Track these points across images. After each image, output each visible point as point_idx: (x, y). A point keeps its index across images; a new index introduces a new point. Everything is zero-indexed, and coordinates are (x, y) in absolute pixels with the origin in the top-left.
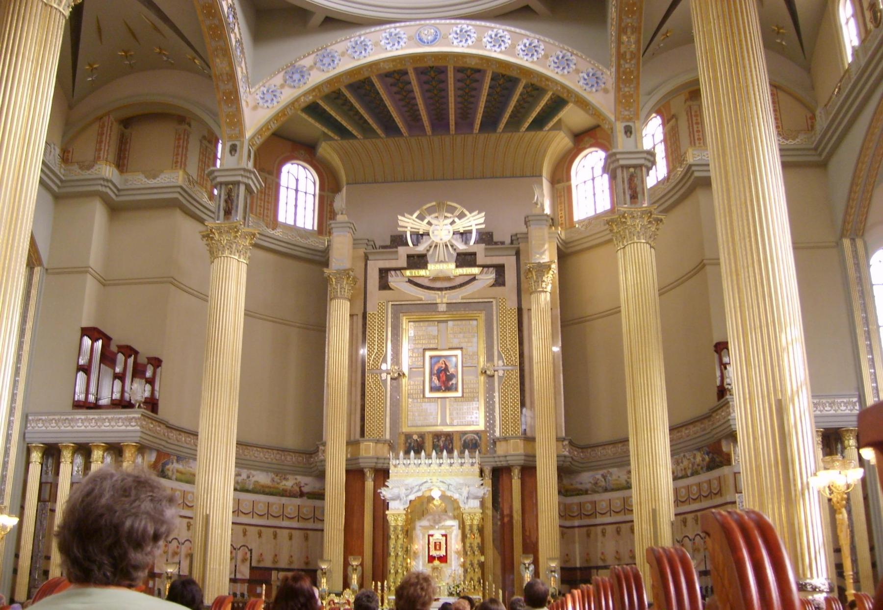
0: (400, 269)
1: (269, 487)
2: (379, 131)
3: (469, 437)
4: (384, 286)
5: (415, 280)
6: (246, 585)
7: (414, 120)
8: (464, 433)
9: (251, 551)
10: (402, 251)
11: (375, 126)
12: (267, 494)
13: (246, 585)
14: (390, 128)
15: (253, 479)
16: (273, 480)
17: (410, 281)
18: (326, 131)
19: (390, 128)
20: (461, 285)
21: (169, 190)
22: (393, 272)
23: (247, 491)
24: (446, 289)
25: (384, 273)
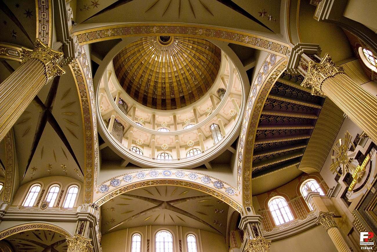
0: (347, 188)
2: (304, 146)
5: (355, 188)
11: (302, 147)
20: (370, 171)
21: (300, 227)
24: (367, 179)
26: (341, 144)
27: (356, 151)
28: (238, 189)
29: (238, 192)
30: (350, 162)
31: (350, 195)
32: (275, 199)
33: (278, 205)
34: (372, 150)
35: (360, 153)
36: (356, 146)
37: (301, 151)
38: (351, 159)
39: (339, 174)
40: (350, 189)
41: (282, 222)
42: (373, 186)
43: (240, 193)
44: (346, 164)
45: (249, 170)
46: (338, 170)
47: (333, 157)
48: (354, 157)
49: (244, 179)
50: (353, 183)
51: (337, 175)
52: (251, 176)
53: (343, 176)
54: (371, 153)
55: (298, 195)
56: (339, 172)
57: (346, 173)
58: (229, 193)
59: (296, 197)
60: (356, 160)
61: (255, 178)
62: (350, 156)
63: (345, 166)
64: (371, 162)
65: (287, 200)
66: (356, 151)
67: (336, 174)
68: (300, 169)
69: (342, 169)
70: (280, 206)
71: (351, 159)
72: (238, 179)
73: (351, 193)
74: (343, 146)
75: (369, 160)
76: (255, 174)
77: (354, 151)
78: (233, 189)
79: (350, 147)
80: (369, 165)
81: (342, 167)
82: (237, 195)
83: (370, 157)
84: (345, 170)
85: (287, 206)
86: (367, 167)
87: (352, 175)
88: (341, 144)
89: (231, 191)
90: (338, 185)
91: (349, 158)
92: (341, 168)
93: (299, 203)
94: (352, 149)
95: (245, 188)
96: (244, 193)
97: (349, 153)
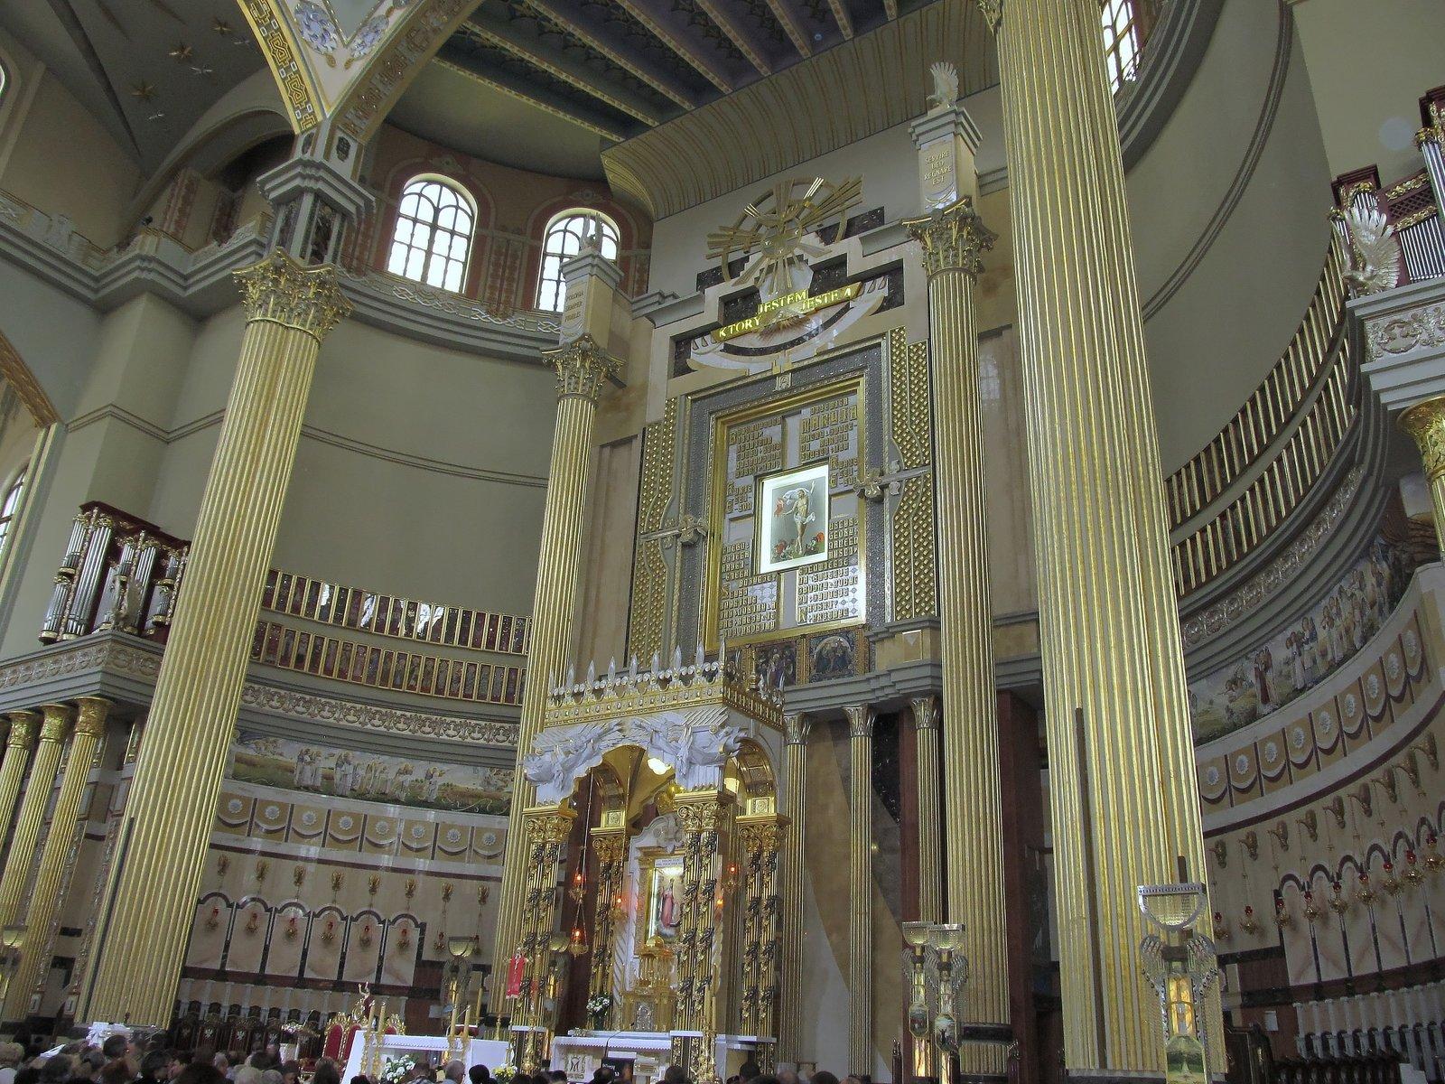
1: (477, 796)
2: (686, 106)
3: (832, 642)
4: (680, 368)
6: (404, 999)
7: (735, 66)
8: (821, 636)
9: (422, 927)
10: (714, 293)
12: (471, 810)
13: (404, 999)
14: (699, 89)
15: (440, 781)
16: (487, 782)
17: (730, 349)
18: (605, 133)
19: (699, 89)
22: (698, 341)
23: (426, 804)
25: (682, 344)
26: (810, 193)
27: (836, 249)
28: (354, 45)
29: (342, 56)
30: (791, 262)
31: (707, 349)
32: (442, 184)
33: (437, 211)
34: (879, 281)
35: (841, 262)
36: (847, 235)
37: (663, 108)
38: (800, 257)
39: (725, 272)
40: (722, 333)
41: (414, 274)
42: (793, 371)
43: (348, 64)
44: (773, 261)
45: (452, 13)
46: (733, 257)
47: (750, 210)
48: (813, 261)
49: (409, 33)
50: (748, 324)
51: (718, 269)
52: (439, 41)
53: (735, 285)
54: (868, 284)
55: (529, 231)
56: (730, 265)
57: (750, 283)
58: (306, 32)
59: (520, 232)
60: (810, 275)
61: (446, 65)
62: (804, 247)
63: (764, 265)
64: (847, 309)
65: (483, 221)
66: (836, 249)
67: (717, 262)
68: (605, 161)
69: (747, 266)
70: (445, 219)
71: (800, 257)
72: (382, 11)
73: (711, 346)
74: (811, 206)
75: (848, 299)
76: (460, 50)
77: (827, 244)
78: (330, 27)
79: (827, 223)
80: (832, 312)
81: (753, 259)
82: (331, 61)
83: (857, 295)
84: (757, 274)
85: (469, 238)
86: (821, 313)
87: (760, 302)
88: (810, 193)
89: (317, 29)
90: (699, 299)
91: (797, 252)
92: (747, 259)
93: (515, 257)
94: (827, 235)
95: (388, 64)
96: (367, 77)
97: (812, 240)
